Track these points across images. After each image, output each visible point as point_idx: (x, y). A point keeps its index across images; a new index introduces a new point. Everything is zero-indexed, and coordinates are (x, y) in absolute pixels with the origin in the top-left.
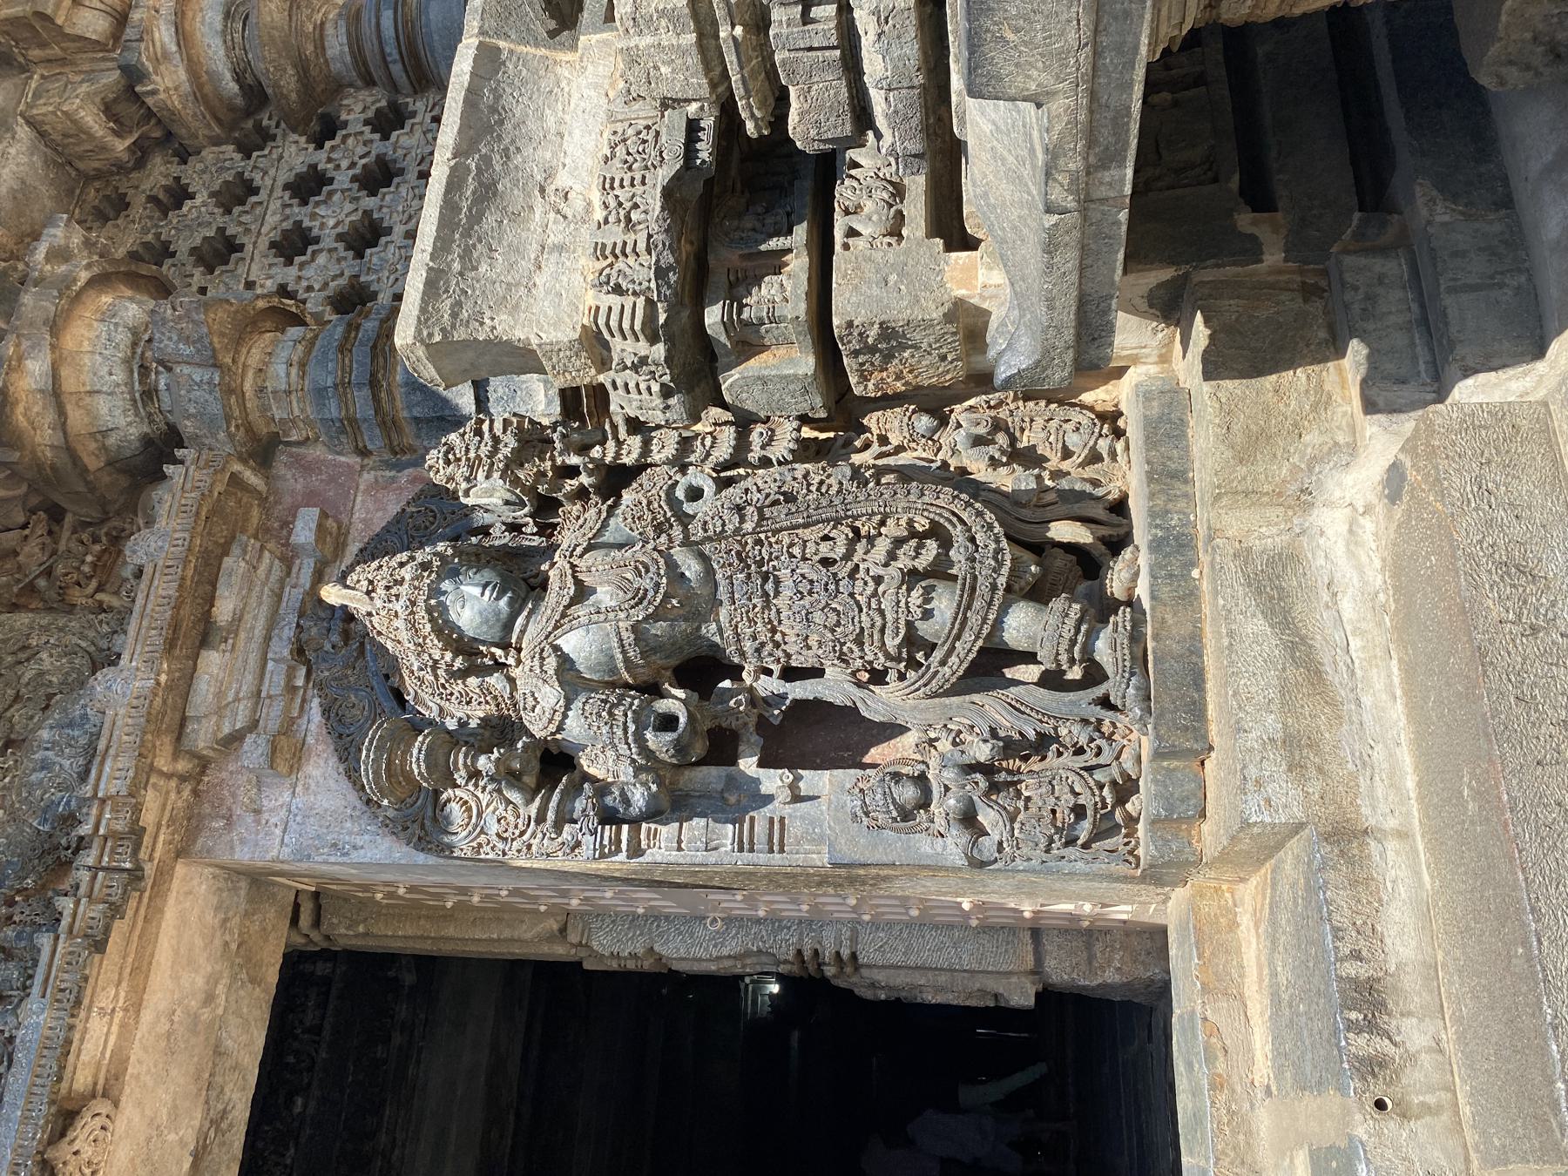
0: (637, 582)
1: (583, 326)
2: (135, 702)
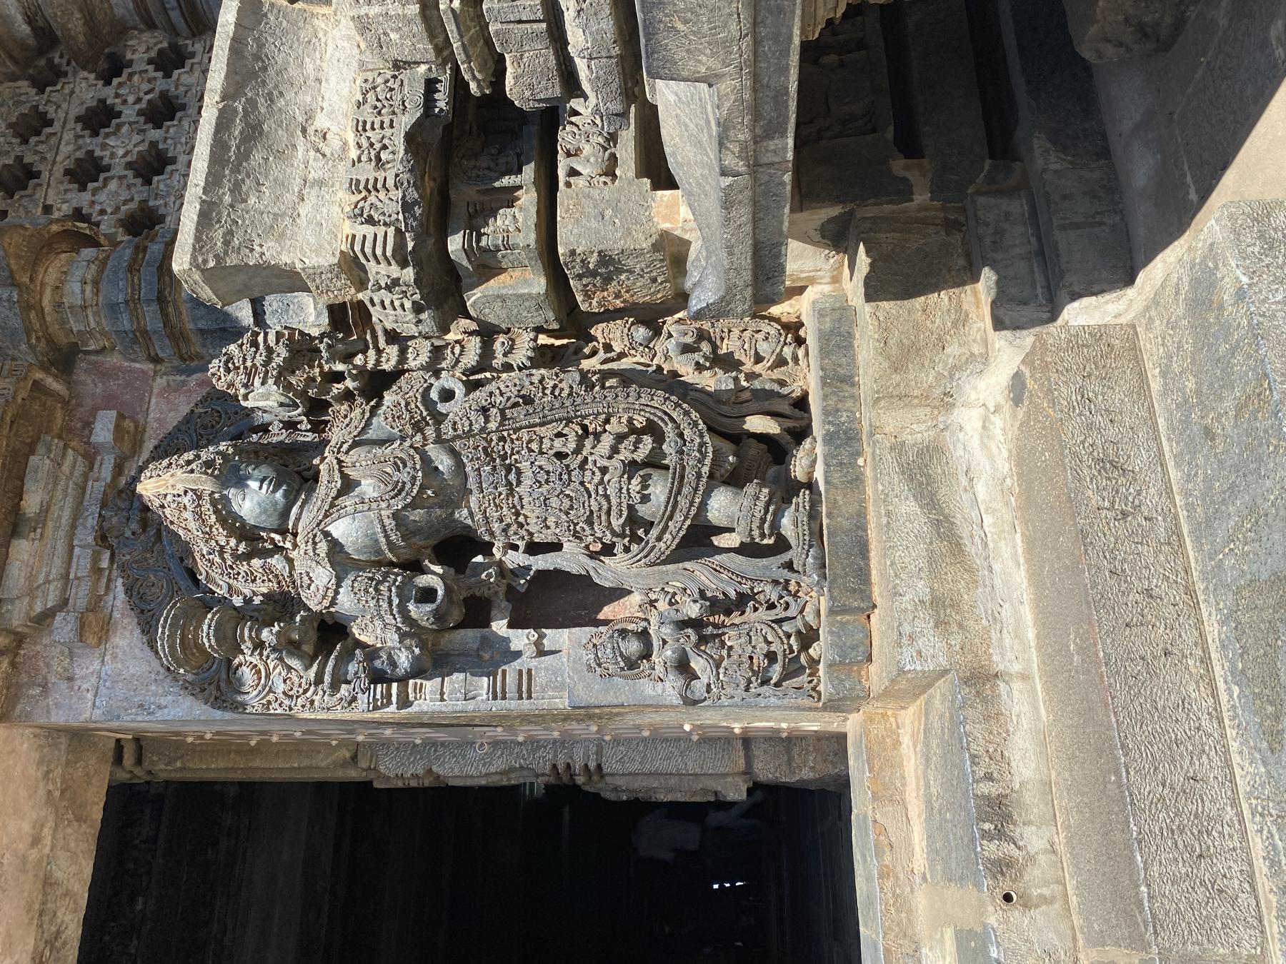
1: (342, 252)
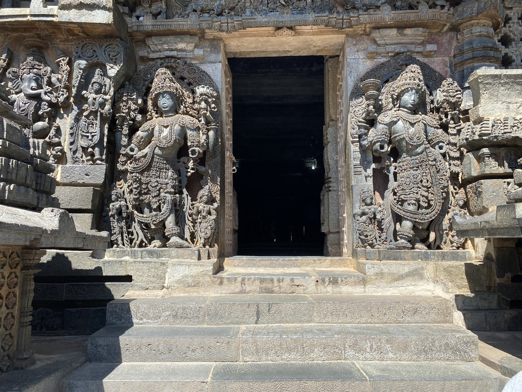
0: (415, 138)
2: (382, 18)
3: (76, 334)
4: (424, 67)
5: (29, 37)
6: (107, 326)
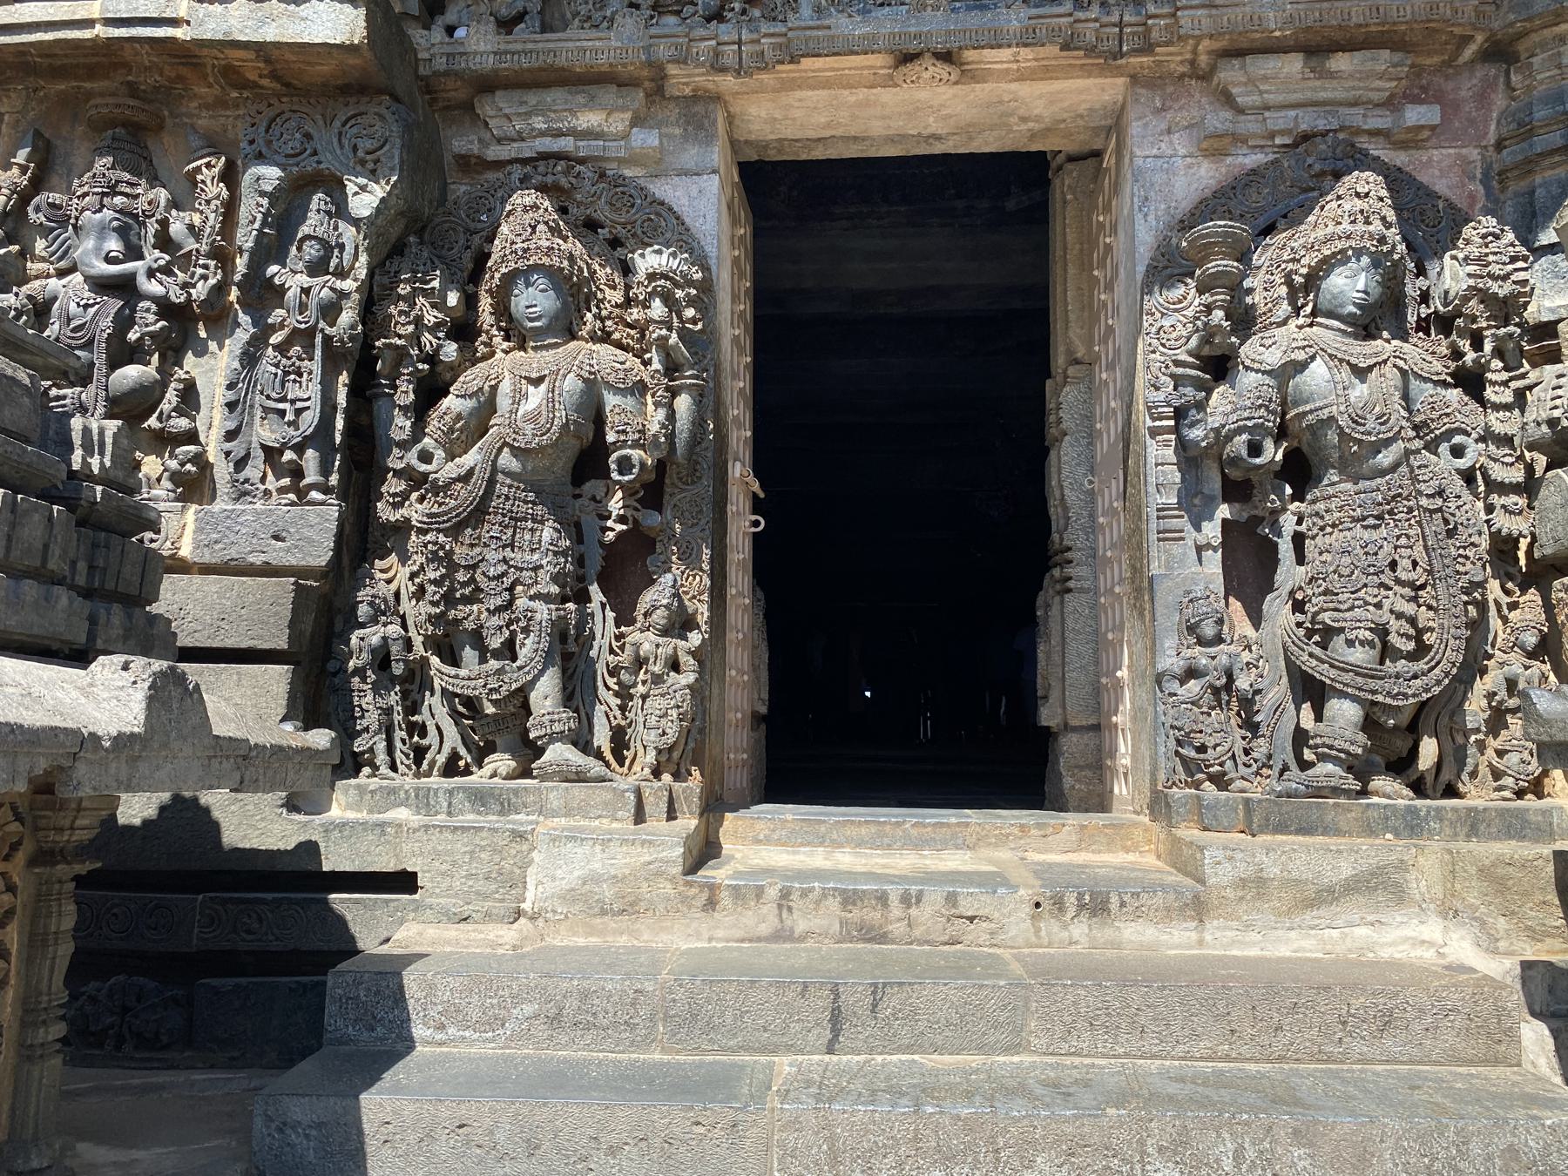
3: (232, 1064)
4: (1397, 181)
5: (102, 95)
6: (325, 1050)
